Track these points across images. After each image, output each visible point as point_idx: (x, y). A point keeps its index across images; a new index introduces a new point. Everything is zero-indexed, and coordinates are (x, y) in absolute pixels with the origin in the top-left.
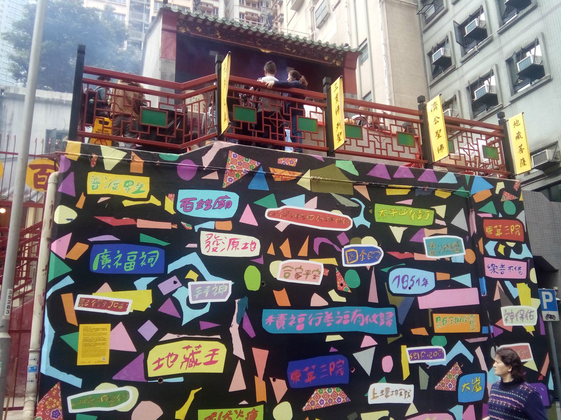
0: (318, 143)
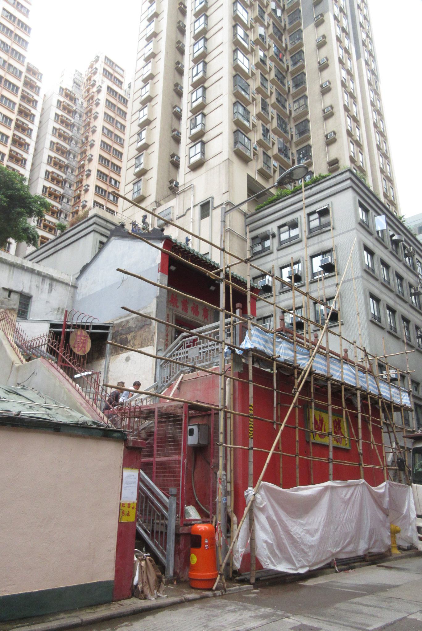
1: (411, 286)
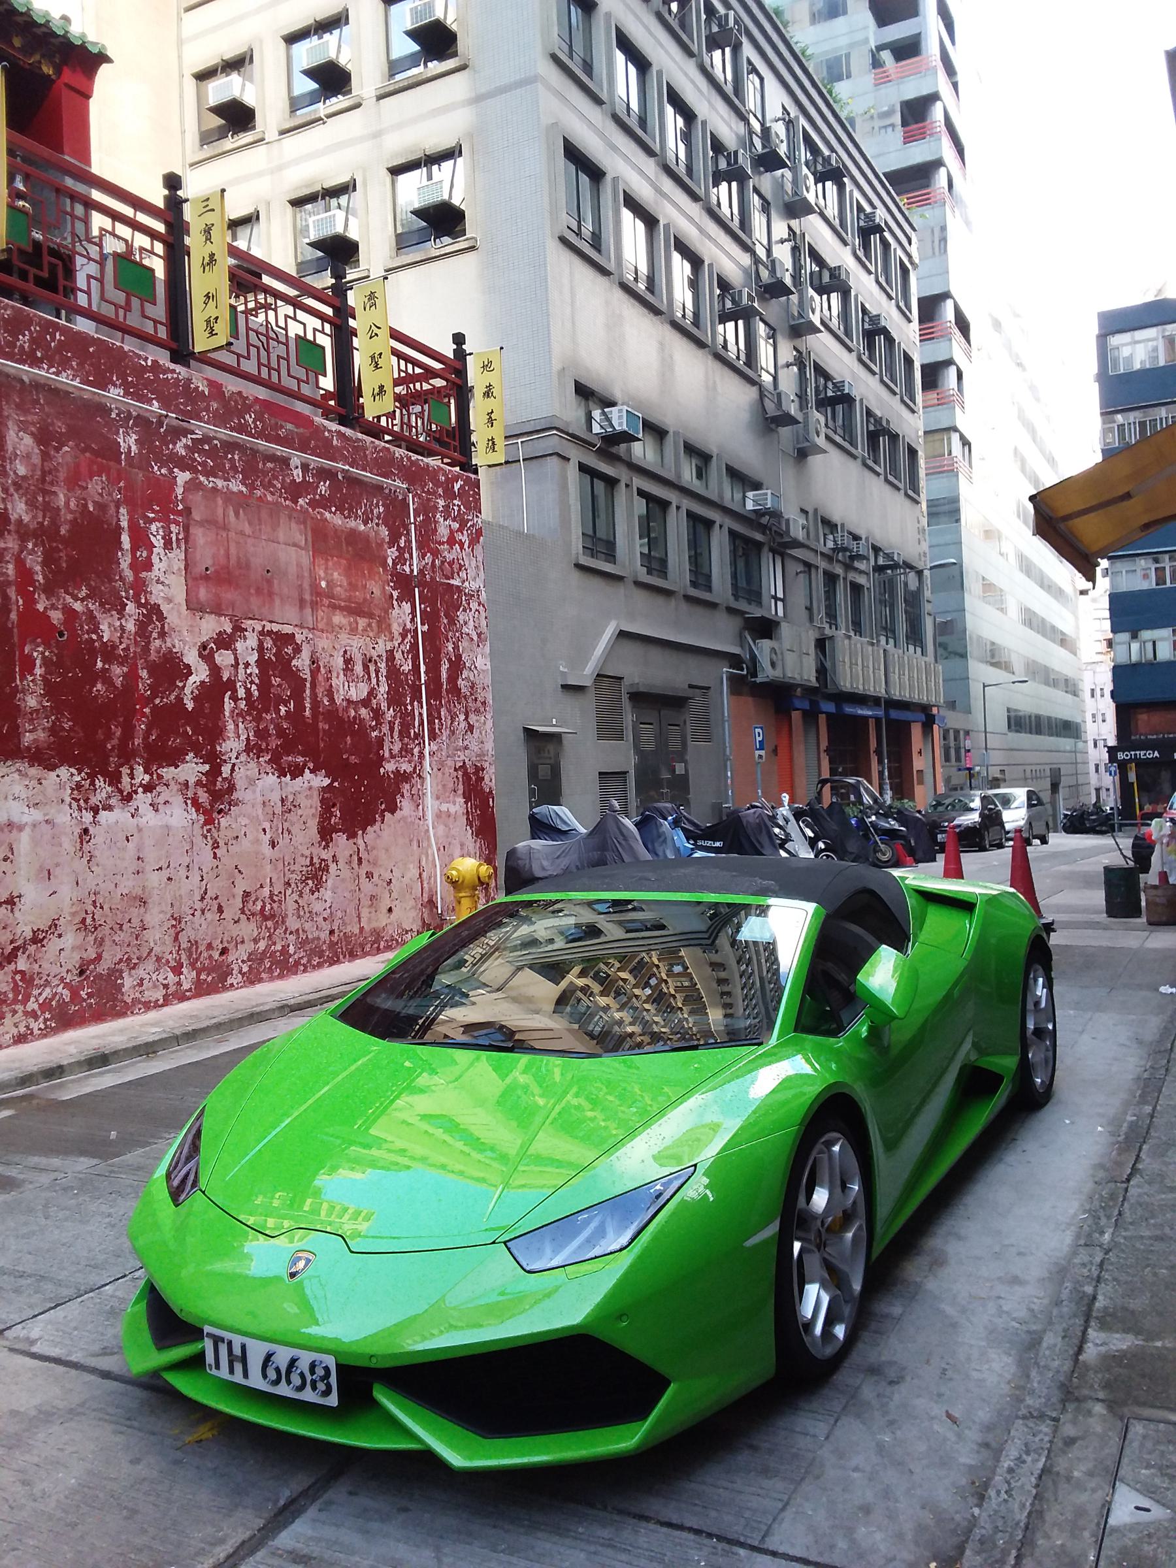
0: (155, 328)
1: (718, 146)
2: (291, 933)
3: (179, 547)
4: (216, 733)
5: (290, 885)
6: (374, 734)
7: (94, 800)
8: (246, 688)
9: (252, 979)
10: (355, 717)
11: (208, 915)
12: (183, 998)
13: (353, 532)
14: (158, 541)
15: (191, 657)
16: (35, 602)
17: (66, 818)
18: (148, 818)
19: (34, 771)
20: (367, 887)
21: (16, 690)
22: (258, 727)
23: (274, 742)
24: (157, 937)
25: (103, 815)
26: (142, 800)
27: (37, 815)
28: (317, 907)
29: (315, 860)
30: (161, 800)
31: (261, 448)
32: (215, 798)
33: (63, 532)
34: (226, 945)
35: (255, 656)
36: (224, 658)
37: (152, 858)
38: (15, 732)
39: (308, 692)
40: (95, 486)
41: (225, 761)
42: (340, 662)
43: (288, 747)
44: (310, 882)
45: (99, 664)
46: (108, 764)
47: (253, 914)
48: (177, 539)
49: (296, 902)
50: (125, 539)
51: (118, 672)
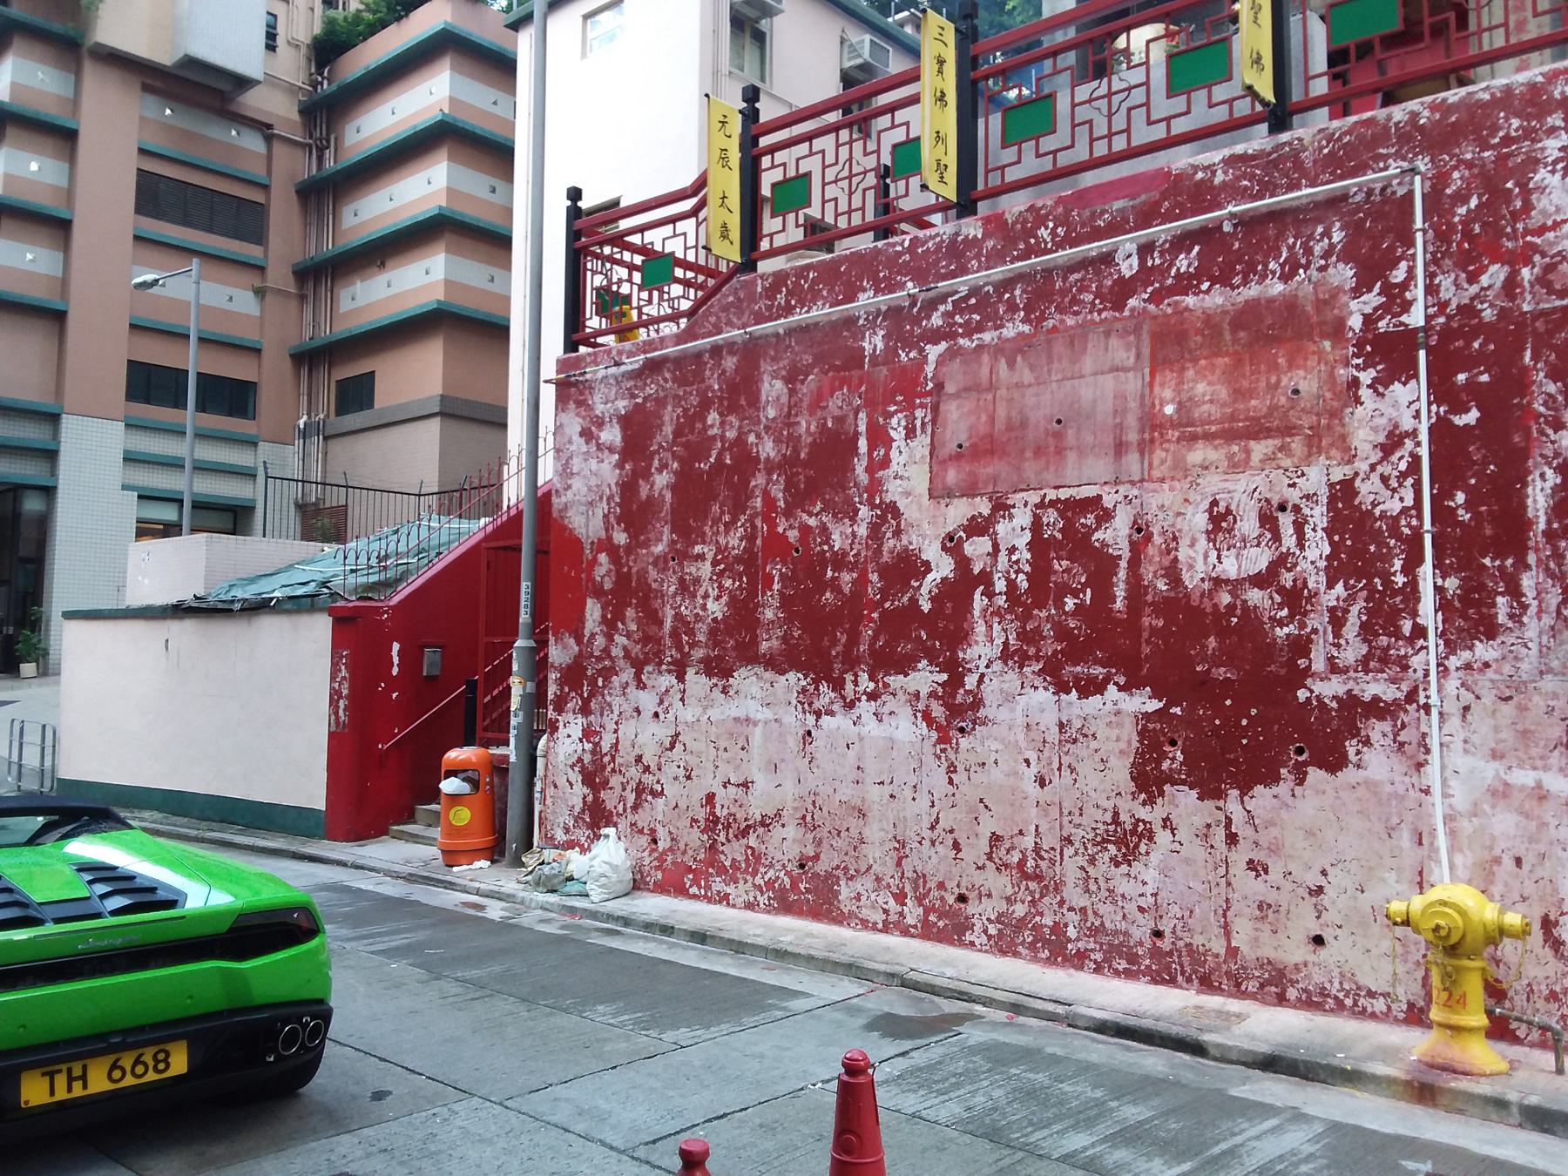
2: (1071, 909)
3: (923, 431)
4: (959, 636)
5: (1071, 843)
6: (1281, 632)
7: (817, 705)
8: (1007, 579)
9: (1003, 945)
10: (1231, 608)
11: (940, 848)
12: (905, 932)
13: (1252, 306)
14: (898, 435)
15: (932, 552)
16: (777, 525)
17: (793, 719)
18: (870, 726)
19: (769, 675)
20: (1247, 884)
21: (757, 605)
22: (1024, 627)
23: (1050, 647)
24: (877, 853)
25: (825, 719)
26: (865, 708)
27: (767, 714)
28: (1124, 887)
29: (1123, 818)
30: (886, 709)
31: (1060, 261)
32: (955, 713)
33: (803, 455)
34: (964, 891)
35: (1027, 536)
36: (977, 548)
37: (873, 770)
38: (755, 642)
39: (1122, 574)
40: (835, 403)
41: (970, 670)
42: (1201, 521)
43: (1076, 650)
44: (1112, 848)
45: (829, 573)
46: (832, 670)
47: (1006, 866)
48: (923, 424)
49: (1082, 868)
50: (863, 444)
51: (846, 578)
